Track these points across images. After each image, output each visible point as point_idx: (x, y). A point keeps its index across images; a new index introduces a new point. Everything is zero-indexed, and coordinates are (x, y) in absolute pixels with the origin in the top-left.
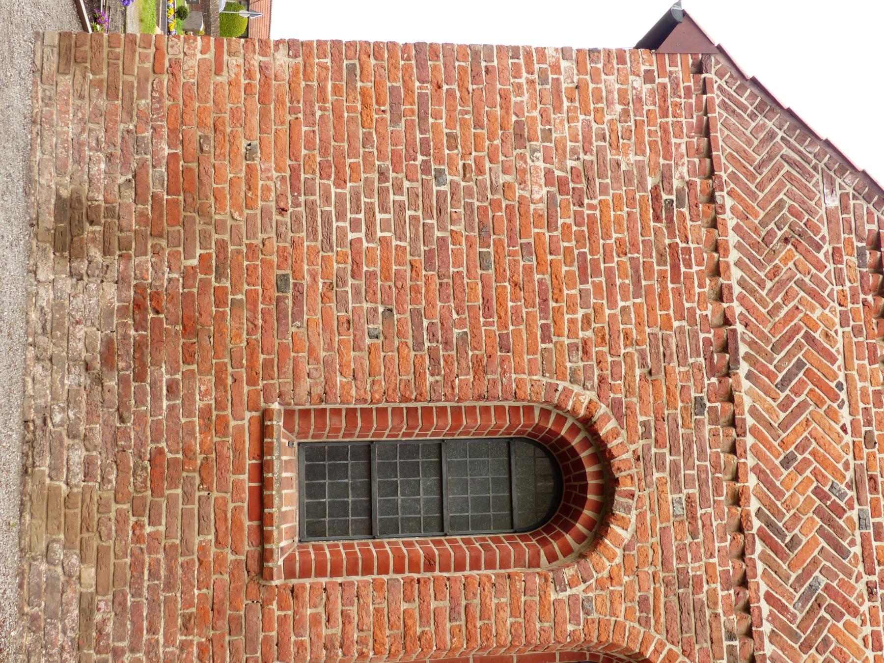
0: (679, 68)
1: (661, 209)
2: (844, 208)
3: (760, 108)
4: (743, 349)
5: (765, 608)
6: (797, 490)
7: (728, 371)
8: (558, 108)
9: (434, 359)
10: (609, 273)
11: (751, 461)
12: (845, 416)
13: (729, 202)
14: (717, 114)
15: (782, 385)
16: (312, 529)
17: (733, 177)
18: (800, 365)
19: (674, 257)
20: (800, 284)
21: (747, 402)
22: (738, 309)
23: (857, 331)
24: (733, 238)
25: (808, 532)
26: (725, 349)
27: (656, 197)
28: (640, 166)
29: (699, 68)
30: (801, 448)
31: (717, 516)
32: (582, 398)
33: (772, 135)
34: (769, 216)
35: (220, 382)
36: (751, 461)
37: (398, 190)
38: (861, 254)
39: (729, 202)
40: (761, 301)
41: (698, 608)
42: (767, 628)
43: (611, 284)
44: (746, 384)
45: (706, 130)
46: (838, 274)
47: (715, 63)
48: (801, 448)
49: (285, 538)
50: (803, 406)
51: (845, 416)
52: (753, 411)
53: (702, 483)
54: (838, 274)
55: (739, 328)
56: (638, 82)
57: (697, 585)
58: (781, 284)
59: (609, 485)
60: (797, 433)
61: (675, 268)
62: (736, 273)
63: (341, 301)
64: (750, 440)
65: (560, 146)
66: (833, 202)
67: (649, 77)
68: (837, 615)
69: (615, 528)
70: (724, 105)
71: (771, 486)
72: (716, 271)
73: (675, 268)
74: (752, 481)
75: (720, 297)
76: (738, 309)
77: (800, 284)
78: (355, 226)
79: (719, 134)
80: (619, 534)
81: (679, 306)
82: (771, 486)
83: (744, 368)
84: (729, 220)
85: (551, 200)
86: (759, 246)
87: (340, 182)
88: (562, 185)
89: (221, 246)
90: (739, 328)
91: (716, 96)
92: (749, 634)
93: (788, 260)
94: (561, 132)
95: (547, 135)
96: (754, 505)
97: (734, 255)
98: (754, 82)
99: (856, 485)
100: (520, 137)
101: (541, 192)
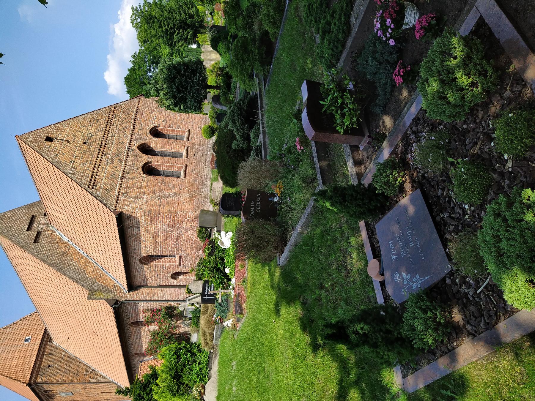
1: (127, 194)
14: (114, 204)
25: (116, 160)
29: (115, 210)
32: (144, 175)
45: (117, 202)
56: (126, 208)
60: (114, 170)
67: (124, 208)
75: (121, 184)
79: (115, 201)
84: (116, 192)
85: (144, 195)
88: (142, 197)
93: (108, 187)
100: (146, 203)
101: (145, 196)
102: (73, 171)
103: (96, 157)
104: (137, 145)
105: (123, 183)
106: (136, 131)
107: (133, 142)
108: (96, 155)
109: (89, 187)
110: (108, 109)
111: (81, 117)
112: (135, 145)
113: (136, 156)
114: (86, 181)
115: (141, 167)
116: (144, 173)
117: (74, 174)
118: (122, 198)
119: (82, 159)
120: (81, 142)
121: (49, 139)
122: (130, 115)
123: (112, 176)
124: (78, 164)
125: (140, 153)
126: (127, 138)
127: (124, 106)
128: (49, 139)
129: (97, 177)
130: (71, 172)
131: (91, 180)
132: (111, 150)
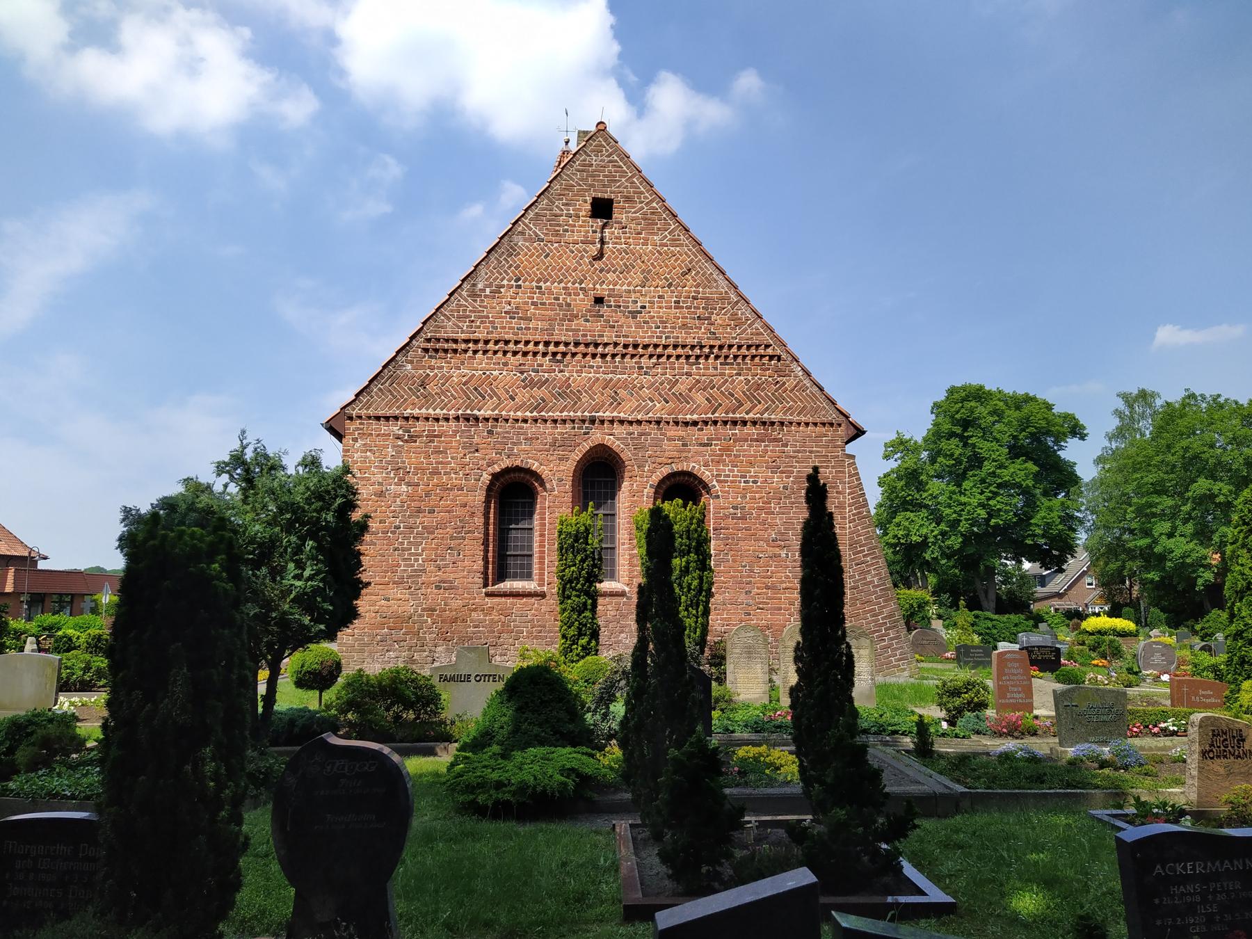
0: (351, 426)
1: (412, 439)
2: (411, 362)
3: (369, 394)
4: (469, 412)
5: (565, 413)
6: (523, 395)
7: (477, 419)
8: (369, 479)
9: (469, 532)
10: (437, 463)
11: (512, 413)
12: (496, 373)
13: (409, 411)
14: (371, 412)
15: (484, 398)
16: (529, 576)
17: (398, 408)
18: (476, 389)
19: (432, 436)
20: (443, 385)
21: (489, 412)
22: (452, 412)
23: (463, 363)
24: (424, 411)
25: (538, 393)
26: (468, 420)
27: (407, 441)
28: (394, 446)
29: (351, 418)
30: (507, 392)
31: (530, 429)
32: (486, 478)
33: (380, 389)
34: (414, 394)
35: (475, 610)
36: (512, 413)
37: (402, 543)
38: (430, 357)
39: (409, 411)
40: (450, 401)
41: (564, 439)
42: (572, 414)
43: (441, 463)
44: (482, 412)
45: (378, 418)
46: (439, 368)
47: (349, 411)
48: (507, 392)
49: (531, 586)
50: (492, 390)
51: (496, 373)
52: (493, 410)
53: (519, 433)
54: (439, 368)
55: (460, 412)
56: (357, 445)
57: (555, 440)
58: (442, 392)
59: (518, 469)
60: (501, 392)
61: (436, 436)
62: (438, 411)
63: (446, 566)
64: (504, 413)
65: (385, 479)
66: (409, 367)
67: (355, 440)
68: (569, 386)
69: (534, 468)
70: (368, 409)
71: (521, 406)
72: (437, 420)
73: (436, 436)
74: (519, 413)
75: (447, 420)
76: (452, 412)
77: (443, 385)
78: (417, 560)
79: (381, 413)
80: (535, 466)
81: (451, 436)
82: (521, 406)
83: (476, 412)
84: (416, 412)
85: (408, 484)
86: (428, 399)
87: (399, 565)
88: (401, 480)
89: (423, 610)
90: (460, 412)
91: (363, 412)
92: (573, 421)
93: (432, 388)
94: (379, 478)
95: (380, 484)
96: (528, 414)
97: (431, 411)
98: (357, 395)
99: (522, 373)
101: (404, 488)
102: (484, 290)
103: (546, 338)
104: (609, 440)
105: (453, 423)
106: (680, 431)
107: (618, 429)
108: (556, 338)
109: (429, 340)
110: (767, 338)
111: (711, 270)
112: (614, 438)
113: (565, 444)
114: (449, 328)
115: (518, 463)
116: (493, 475)
117: (473, 295)
118: (395, 428)
119: (533, 303)
120: (603, 290)
121: (602, 209)
122: (748, 405)
123: (478, 389)
124: (510, 298)
125: (577, 455)
126: (638, 409)
127: (790, 383)
128: (602, 209)
129: (470, 353)
130: (480, 286)
131: (456, 341)
132: (580, 374)
